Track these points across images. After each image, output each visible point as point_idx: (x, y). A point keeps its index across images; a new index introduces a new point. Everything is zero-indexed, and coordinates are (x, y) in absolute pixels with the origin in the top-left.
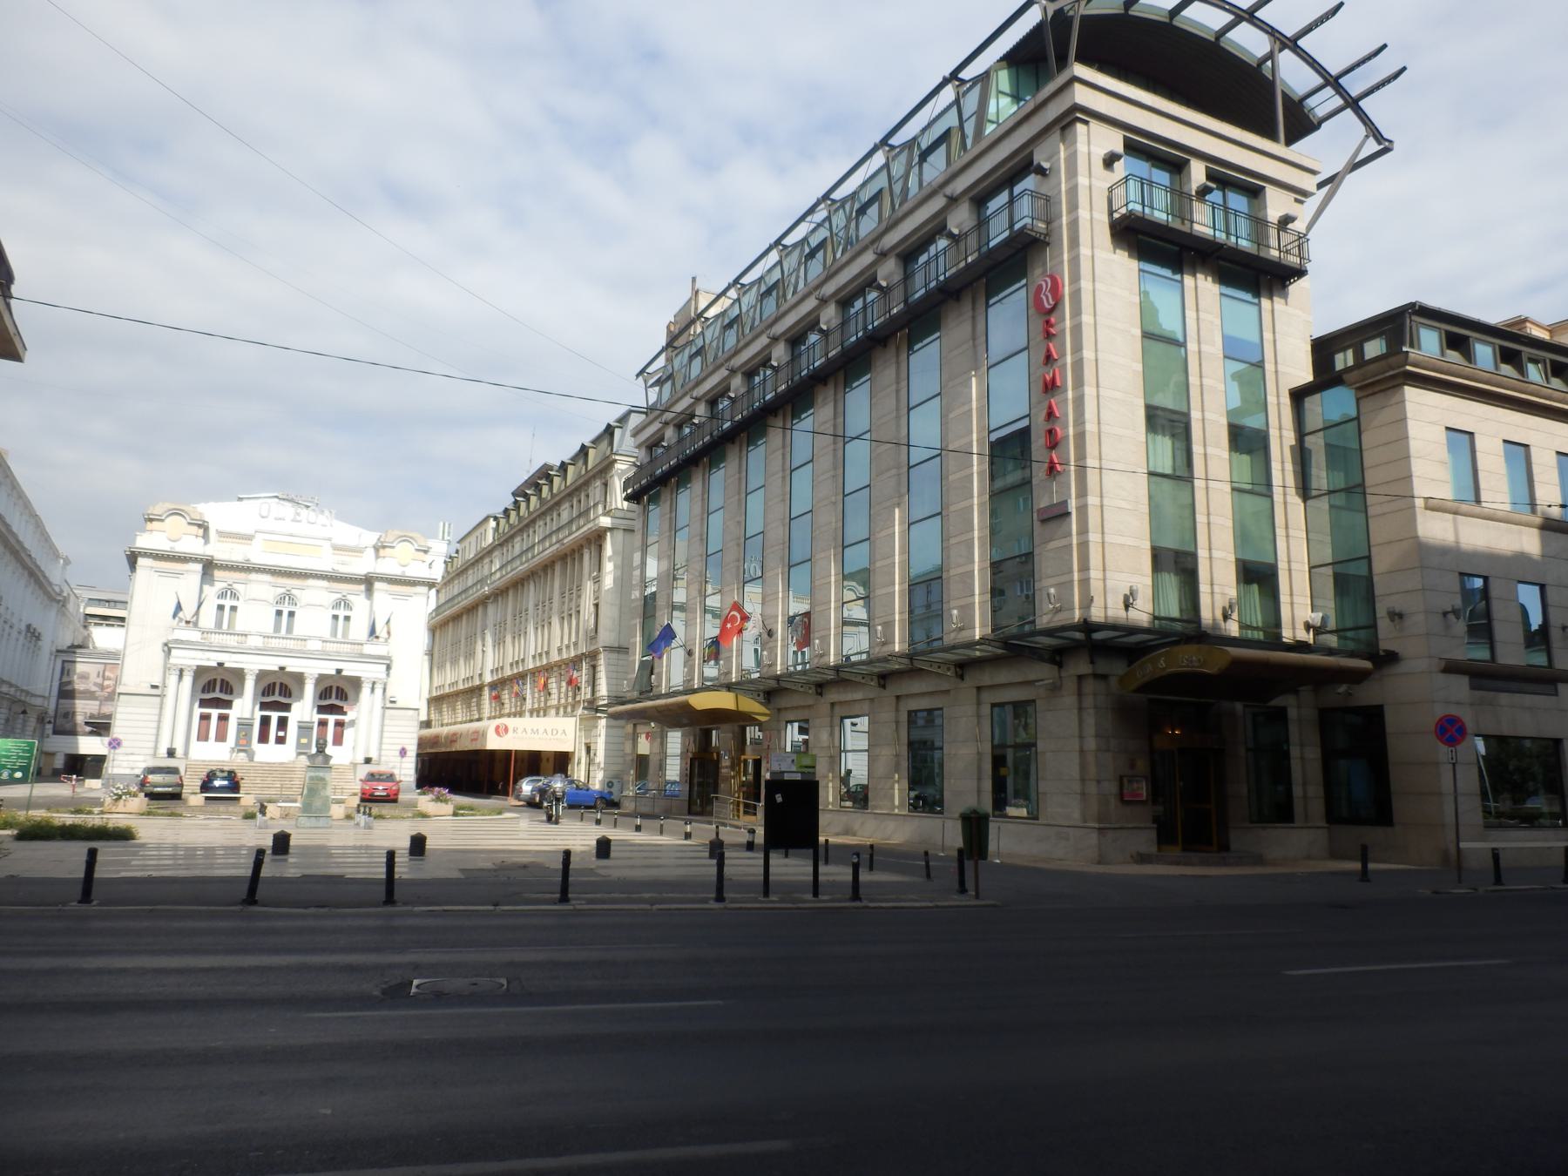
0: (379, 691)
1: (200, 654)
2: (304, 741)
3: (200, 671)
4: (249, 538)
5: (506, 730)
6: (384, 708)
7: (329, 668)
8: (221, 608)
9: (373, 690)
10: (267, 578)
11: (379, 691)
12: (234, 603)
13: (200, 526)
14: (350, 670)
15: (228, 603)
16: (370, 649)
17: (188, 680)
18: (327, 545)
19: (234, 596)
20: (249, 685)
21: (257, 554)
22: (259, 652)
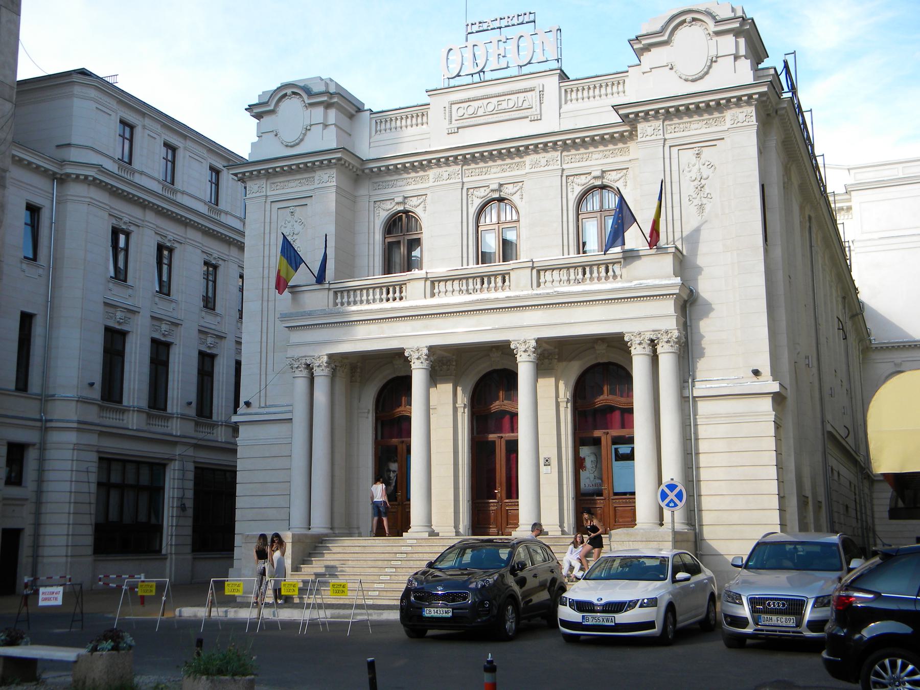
9: (654, 359)
13: (328, 106)
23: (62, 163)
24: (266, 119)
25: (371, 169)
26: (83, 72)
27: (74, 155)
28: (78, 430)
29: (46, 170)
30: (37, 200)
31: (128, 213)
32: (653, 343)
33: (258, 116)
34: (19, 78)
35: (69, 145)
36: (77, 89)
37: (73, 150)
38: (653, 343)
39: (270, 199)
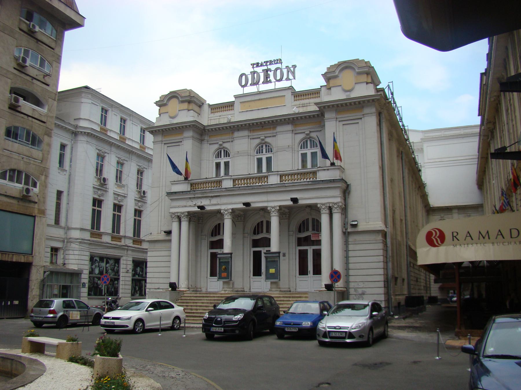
0: (337, 217)
1: (190, 203)
2: (272, 271)
3: (191, 216)
4: (229, 106)
5: (442, 237)
6: (346, 234)
7: (285, 200)
8: (218, 165)
10: (246, 133)
11: (337, 217)
12: (227, 159)
13: (189, 102)
14: (306, 198)
15: (222, 161)
16: (322, 176)
17: (185, 225)
18: (288, 94)
19: (227, 154)
20: (228, 224)
21: (237, 116)
22: (230, 192)
23: (76, 127)
24: (162, 108)
25: (208, 130)
26: (87, 87)
27: (83, 124)
28: (80, 242)
29: (69, 130)
30: (65, 142)
31: (105, 148)
32: (330, 209)
33: (160, 106)
34: (59, 91)
35: (80, 119)
36: (83, 95)
37: (81, 121)
38: (330, 209)
39: (164, 142)
